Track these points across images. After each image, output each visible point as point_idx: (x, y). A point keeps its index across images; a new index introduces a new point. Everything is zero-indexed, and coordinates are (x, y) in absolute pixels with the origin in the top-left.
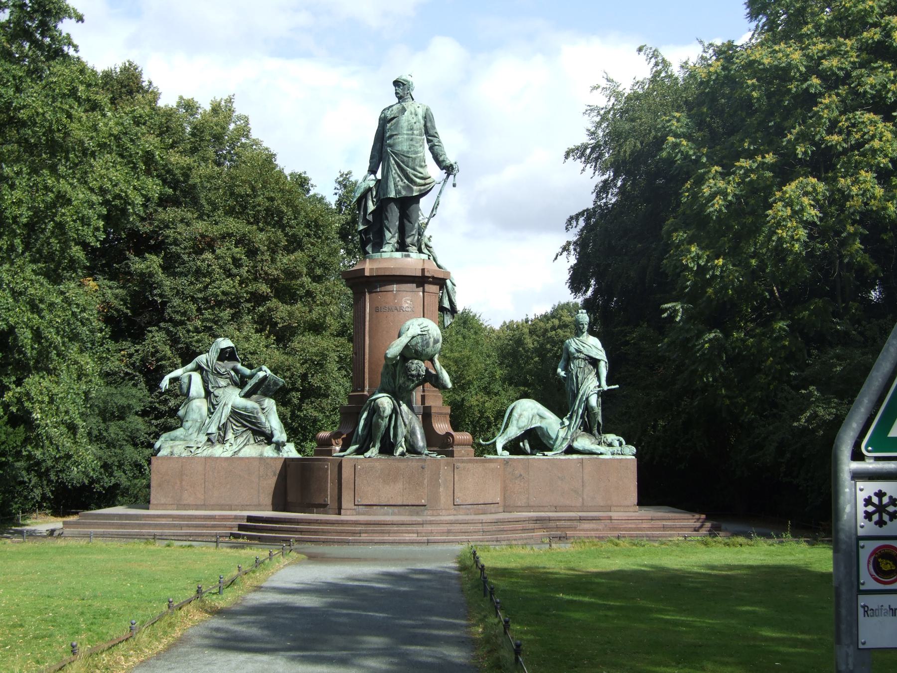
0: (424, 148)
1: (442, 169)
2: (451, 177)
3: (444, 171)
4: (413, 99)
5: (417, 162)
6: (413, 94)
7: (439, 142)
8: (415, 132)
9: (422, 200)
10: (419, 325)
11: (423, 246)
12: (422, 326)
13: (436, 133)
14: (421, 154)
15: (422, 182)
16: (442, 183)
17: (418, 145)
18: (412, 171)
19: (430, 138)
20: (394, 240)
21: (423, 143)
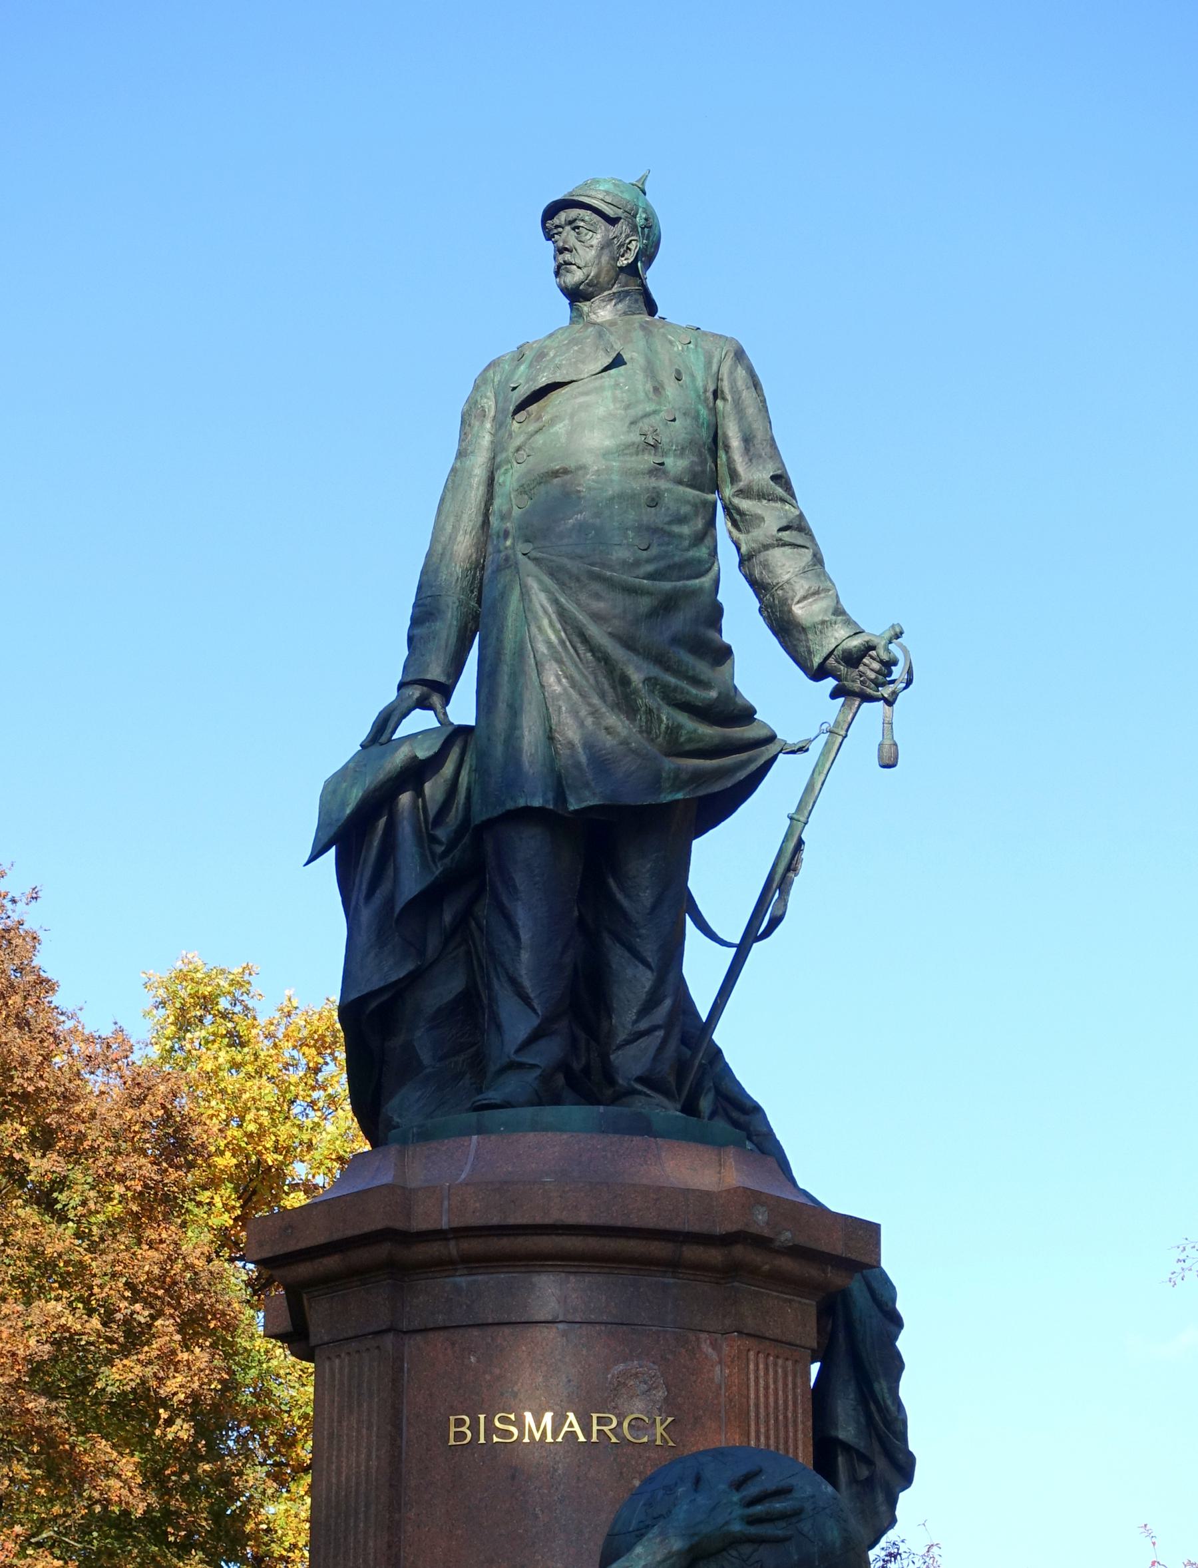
0: (714, 553)
1: (818, 674)
2: (872, 712)
3: (830, 683)
4: (651, 308)
5: (679, 622)
6: (654, 278)
7: (799, 525)
8: (669, 461)
9: (702, 848)
10: (739, 1485)
11: (706, 1104)
12: (753, 1490)
13: (780, 479)
14: (706, 581)
15: (709, 732)
16: (816, 749)
17: (685, 530)
18: (655, 671)
19: (745, 504)
20: (549, 1052)
21: (711, 523)
